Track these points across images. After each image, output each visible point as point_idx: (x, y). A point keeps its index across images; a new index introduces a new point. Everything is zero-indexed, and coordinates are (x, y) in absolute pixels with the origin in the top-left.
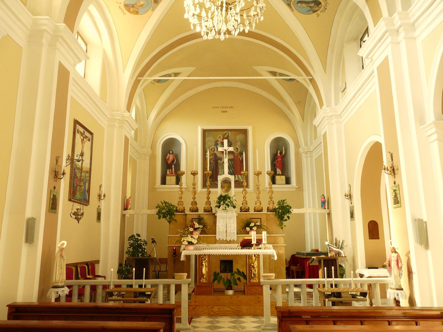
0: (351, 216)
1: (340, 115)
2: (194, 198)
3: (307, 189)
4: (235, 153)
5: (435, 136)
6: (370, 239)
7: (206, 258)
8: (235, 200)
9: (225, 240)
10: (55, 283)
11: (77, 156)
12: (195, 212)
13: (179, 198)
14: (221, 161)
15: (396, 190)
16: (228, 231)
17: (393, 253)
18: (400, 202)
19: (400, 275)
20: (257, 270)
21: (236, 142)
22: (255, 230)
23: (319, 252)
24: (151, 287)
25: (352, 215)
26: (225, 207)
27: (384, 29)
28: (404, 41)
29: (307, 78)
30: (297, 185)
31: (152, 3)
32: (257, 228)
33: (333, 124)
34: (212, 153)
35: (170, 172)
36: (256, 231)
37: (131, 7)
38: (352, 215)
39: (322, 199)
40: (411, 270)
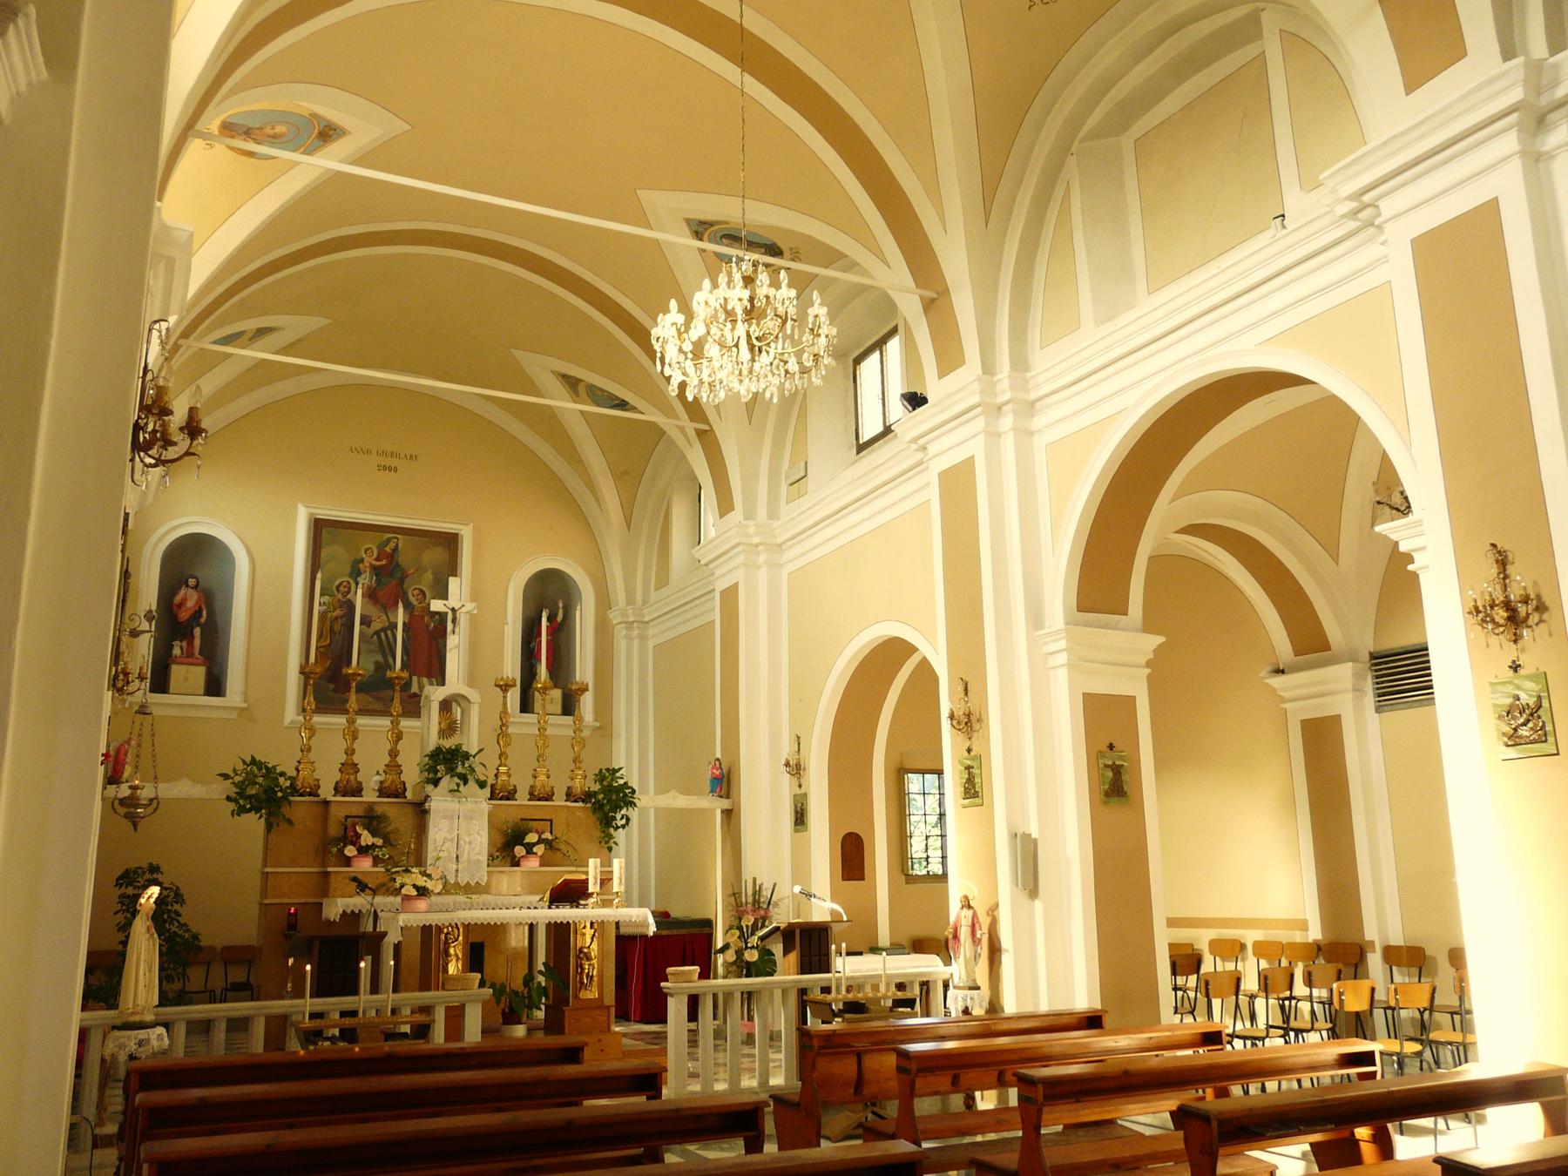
0: (796, 819)
1: (780, 545)
2: (350, 752)
3: (623, 736)
4: (414, 606)
5: (1062, 658)
6: (843, 880)
7: (458, 936)
8: (481, 763)
9: (452, 882)
10: (132, 1013)
11: (134, 616)
12: (353, 796)
13: (302, 751)
14: (369, 627)
15: (973, 767)
16: (464, 858)
17: (965, 909)
18: (980, 794)
19: (976, 956)
20: (596, 966)
21: (420, 570)
22: (540, 853)
23: (670, 920)
24: (412, 1013)
25: (800, 818)
26: (458, 785)
27: (976, 399)
28: (1011, 434)
29: (691, 427)
30: (596, 720)
31: (311, 136)
32: (546, 849)
33: (759, 568)
34: (339, 600)
35: (185, 650)
36: (541, 857)
37: (240, 132)
38: (800, 818)
39: (715, 771)
40: (997, 945)
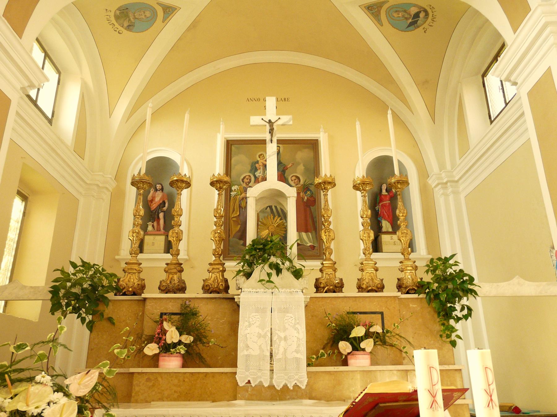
21: (295, 164)
22: (369, 349)
26: (269, 275)
34: (244, 187)
